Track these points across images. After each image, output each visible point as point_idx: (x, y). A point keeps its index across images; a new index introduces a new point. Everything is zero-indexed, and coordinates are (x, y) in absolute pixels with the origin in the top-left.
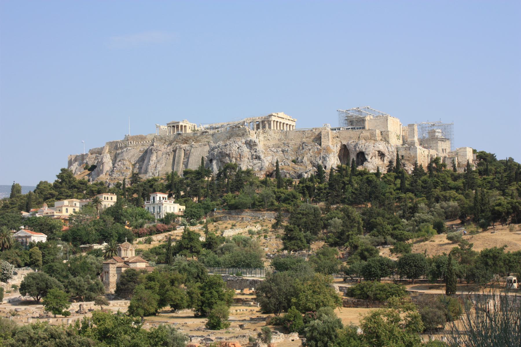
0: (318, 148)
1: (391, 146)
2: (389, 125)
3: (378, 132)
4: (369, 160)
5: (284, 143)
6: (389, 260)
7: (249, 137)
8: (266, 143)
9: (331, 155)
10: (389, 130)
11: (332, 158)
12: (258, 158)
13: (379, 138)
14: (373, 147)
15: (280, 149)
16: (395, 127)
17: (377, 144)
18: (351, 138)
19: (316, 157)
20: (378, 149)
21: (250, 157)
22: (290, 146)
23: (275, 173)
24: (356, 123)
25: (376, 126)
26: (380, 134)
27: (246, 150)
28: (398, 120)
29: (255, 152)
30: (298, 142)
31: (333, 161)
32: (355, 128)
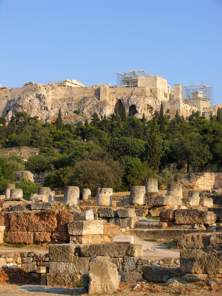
0: (97, 102)
1: (159, 101)
2: (157, 84)
3: (148, 89)
4: (139, 112)
5: (69, 98)
6: (64, 159)
7: (40, 92)
8: (54, 97)
9: (107, 107)
10: (157, 87)
11: (108, 110)
12: (46, 109)
13: (149, 94)
14: (143, 101)
15: (66, 103)
16: (163, 87)
17: (147, 99)
18: (125, 94)
19: (94, 109)
20: (147, 103)
21: (39, 108)
22: (74, 100)
23: (58, 121)
24: (130, 82)
25: (147, 85)
26: (149, 91)
27: (36, 101)
28: (166, 81)
29: (44, 104)
30: (81, 97)
31: (109, 111)
32: (129, 86)
